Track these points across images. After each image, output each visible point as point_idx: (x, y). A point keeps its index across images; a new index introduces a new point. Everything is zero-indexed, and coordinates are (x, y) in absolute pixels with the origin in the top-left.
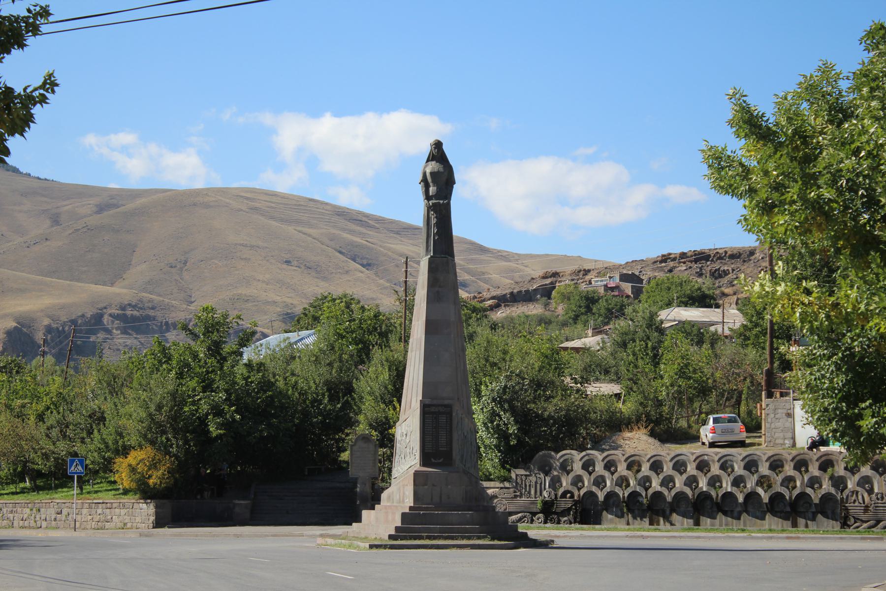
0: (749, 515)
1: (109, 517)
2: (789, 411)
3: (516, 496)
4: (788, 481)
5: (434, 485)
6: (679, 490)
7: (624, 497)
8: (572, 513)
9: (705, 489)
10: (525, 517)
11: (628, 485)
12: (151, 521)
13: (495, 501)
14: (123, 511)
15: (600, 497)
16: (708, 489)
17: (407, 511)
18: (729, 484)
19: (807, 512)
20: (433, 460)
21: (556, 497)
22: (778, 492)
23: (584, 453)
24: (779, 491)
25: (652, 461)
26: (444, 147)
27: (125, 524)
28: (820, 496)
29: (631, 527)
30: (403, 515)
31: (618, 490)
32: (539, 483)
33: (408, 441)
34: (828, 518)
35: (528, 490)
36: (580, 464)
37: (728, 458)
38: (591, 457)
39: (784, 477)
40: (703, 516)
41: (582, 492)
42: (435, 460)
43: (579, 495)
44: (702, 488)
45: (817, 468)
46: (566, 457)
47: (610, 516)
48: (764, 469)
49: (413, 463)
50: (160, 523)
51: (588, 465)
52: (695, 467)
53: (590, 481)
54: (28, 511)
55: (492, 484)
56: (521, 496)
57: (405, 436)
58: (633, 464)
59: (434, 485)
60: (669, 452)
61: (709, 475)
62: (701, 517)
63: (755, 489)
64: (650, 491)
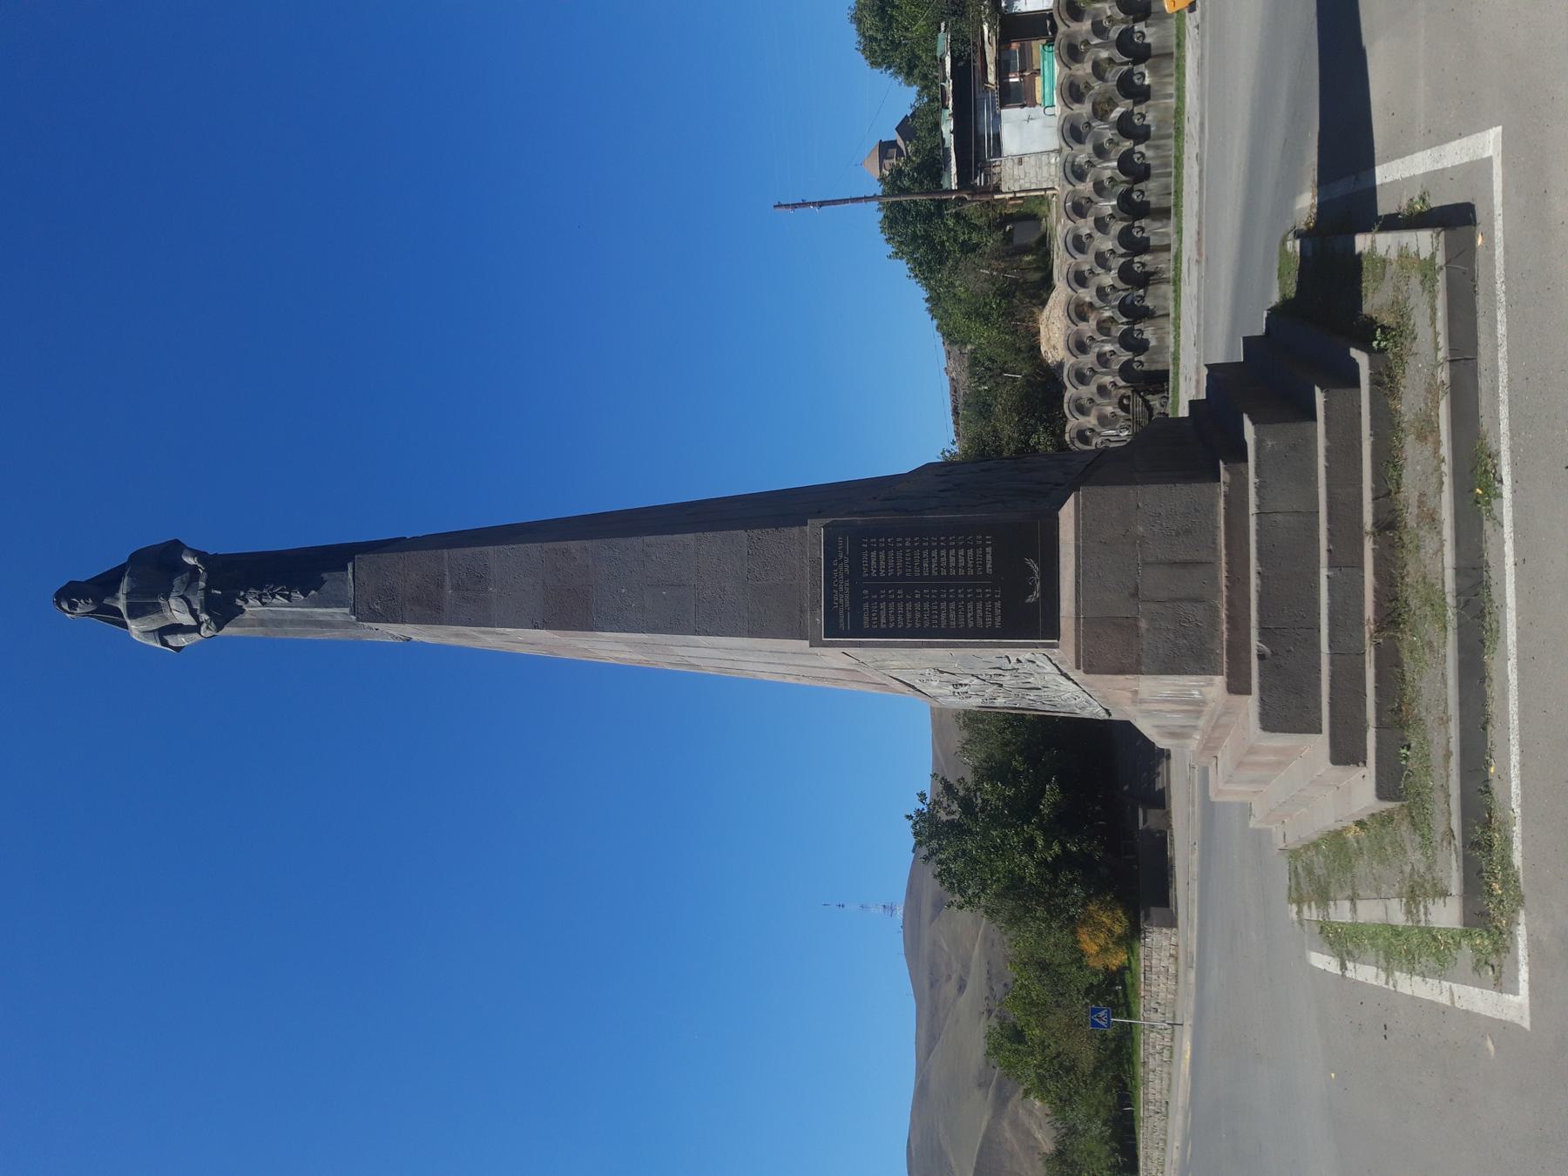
1: (1162, 969)
2: (1016, 161)
4: (1098, 70)
5: (1135, 595)
6: (1117, 242)
7: (1127, 323)
9: (1115, 203)
11: (1112, 319)
12: (1168, 932)
14: (1155, 955)
15: (1126, 358)
17: (1251, 704)
18: (1105, 165)
20: (1037, 594)
22: (1117, 85)
23: (1068, 384)
24: (1115, 83)
26: (83, 577)
27: (1171, 956)
28: (1122, 15)
29: (1172, 310)
30: (1272, 721)
33: (976, 681)
36: (1081, 388)
37: (1068, 170)
39: (1094, 79)
41: (1121, 383)
42: (1032, 588)
43: (1125, 387)
44: (1113, 207)
45: (1080, 24)
48: (1084, 109)
49: (1049, 668)
50: (1171, 922)
51: (1081, 378)
52: (1083, 220)
53: (1105, 372)
54: (1152, 1035)
57: (962, 689)
58: (1079, 312)
59: (1135, 595)
60: (1061, 263)
61: (1095, 197)
64: (1120, 285)
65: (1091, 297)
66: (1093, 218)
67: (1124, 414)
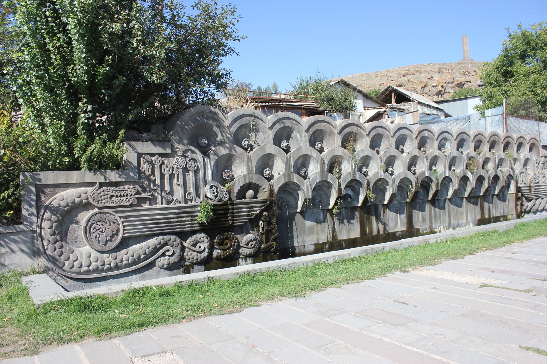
0: (452, 204)
3: (142, 201)
6: (403, 177)
8: (261, 224)
10: (166, 244)
13: (84, 217)
16: (430, 174)
19: (489, 195)
21: (230, 199)
25: (372, 134)
31: (332, 179)
32: (192, 169)
34: (500, 200)
35: (167, 188)
36: (271, 134)
38: (288, 123)
40: (415, 209)
46: (244, 121)
47: (308, 223)
55: (74, 176)
56: (152, 200)
62: (413, 210)
63: (466, 173)
65: (362, 150)
66: (418, 155)
67: (236, 191)
